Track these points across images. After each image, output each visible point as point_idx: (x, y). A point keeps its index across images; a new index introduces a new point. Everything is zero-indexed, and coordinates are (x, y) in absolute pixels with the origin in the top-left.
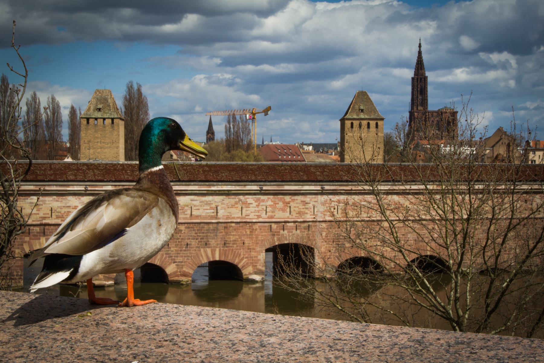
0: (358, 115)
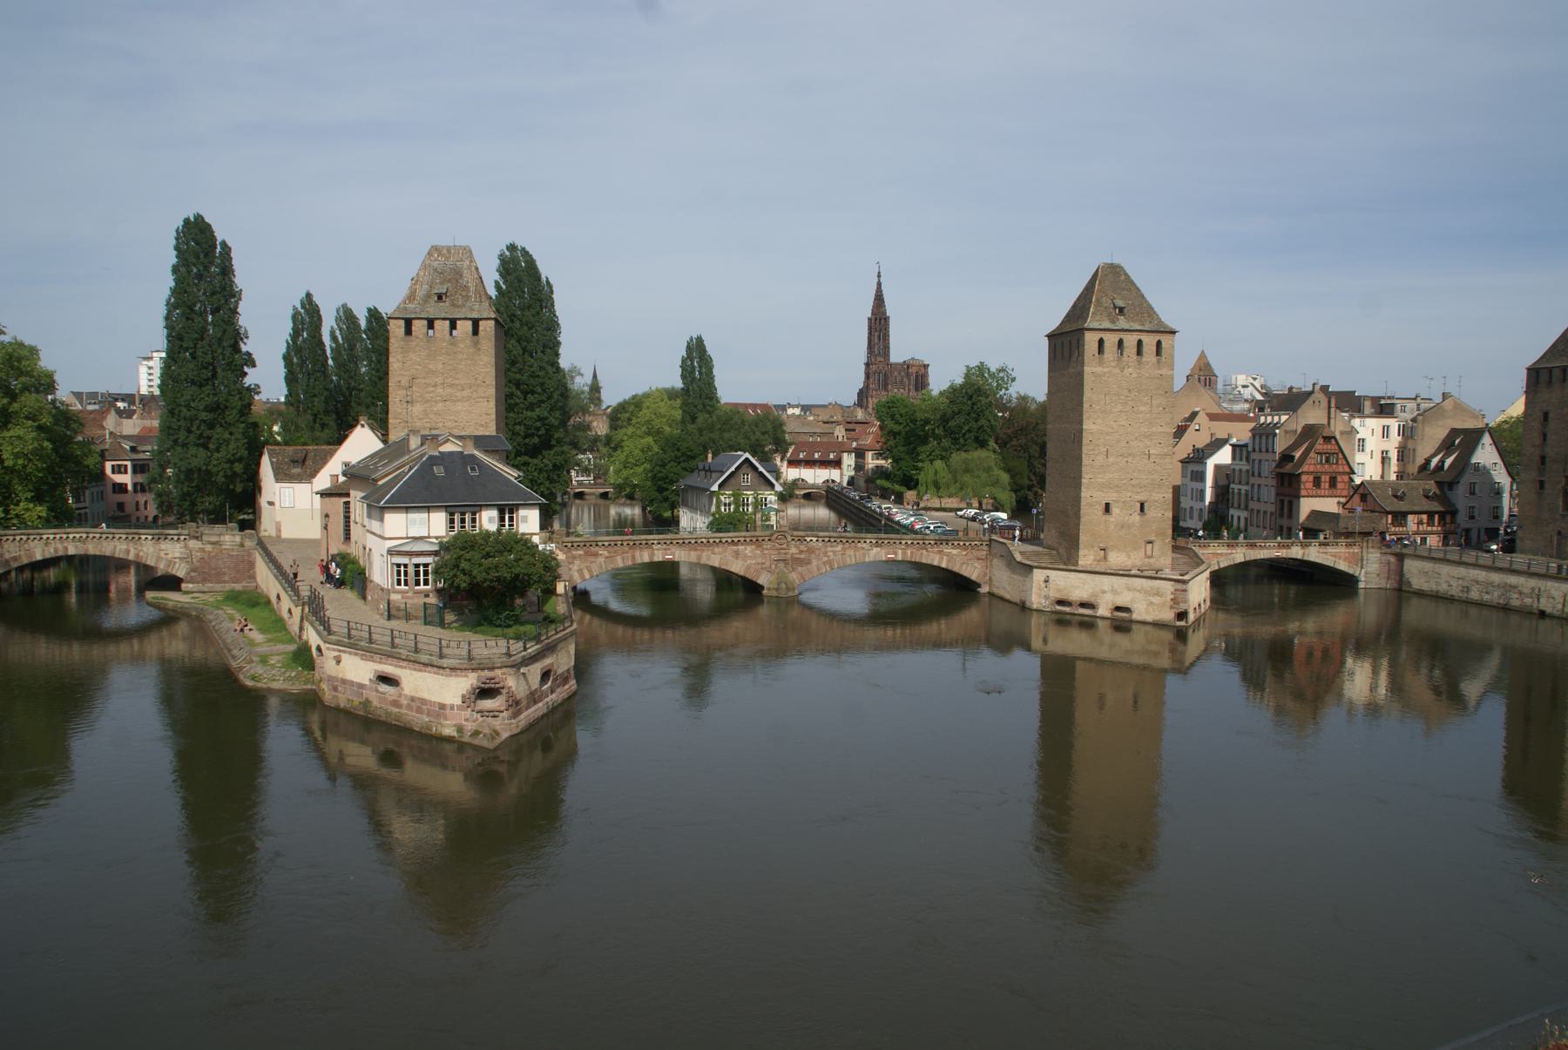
0: (1113, 322)
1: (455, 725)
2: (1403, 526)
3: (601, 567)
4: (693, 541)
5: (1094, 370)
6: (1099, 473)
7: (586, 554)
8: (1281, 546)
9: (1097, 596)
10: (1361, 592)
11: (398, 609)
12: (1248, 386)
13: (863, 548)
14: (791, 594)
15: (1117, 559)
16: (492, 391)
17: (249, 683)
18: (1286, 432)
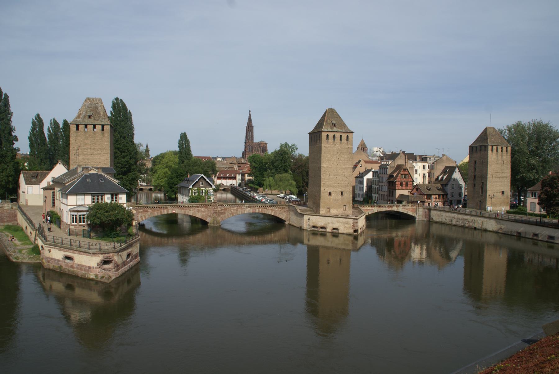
1: (94, 274)
2: (430, 199)
3: (149, 216)
4: (183, 206)
5: (325, 145)
6: (327, 181)
7: (144, 211)
8: (389, 207)
9: (326, 224)
10: (417, 222)
11: (73, 232)
12: (378, 151)
13: (244, 208)
14: (218, 225)
15: (333, 211)
16: (109, 151)
17: (14, 260)
18: (391, 167)
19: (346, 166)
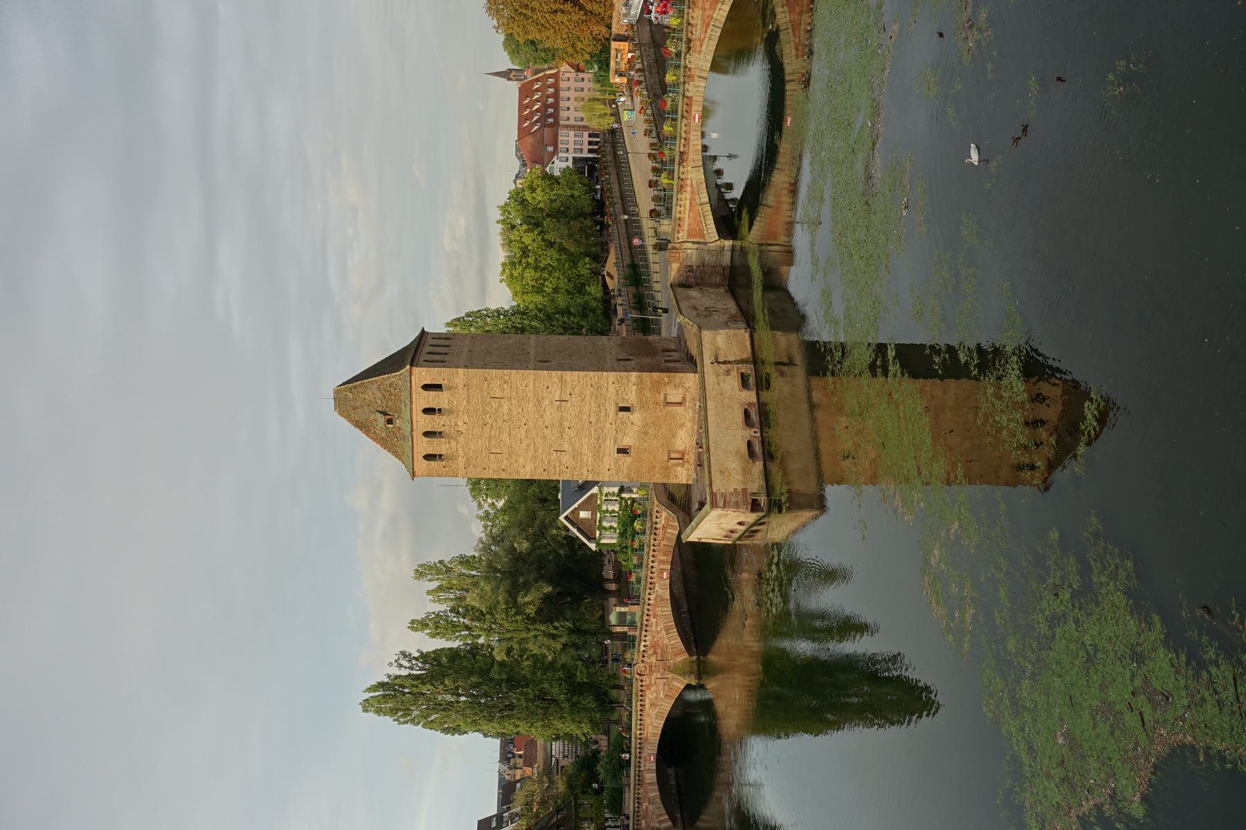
5: (462, 465)
19: (530, 394)
